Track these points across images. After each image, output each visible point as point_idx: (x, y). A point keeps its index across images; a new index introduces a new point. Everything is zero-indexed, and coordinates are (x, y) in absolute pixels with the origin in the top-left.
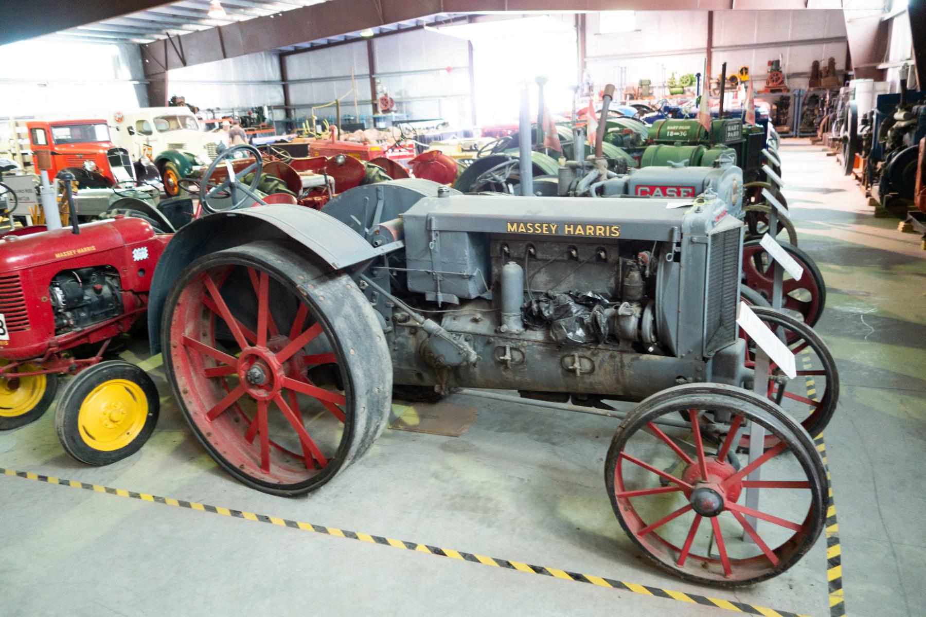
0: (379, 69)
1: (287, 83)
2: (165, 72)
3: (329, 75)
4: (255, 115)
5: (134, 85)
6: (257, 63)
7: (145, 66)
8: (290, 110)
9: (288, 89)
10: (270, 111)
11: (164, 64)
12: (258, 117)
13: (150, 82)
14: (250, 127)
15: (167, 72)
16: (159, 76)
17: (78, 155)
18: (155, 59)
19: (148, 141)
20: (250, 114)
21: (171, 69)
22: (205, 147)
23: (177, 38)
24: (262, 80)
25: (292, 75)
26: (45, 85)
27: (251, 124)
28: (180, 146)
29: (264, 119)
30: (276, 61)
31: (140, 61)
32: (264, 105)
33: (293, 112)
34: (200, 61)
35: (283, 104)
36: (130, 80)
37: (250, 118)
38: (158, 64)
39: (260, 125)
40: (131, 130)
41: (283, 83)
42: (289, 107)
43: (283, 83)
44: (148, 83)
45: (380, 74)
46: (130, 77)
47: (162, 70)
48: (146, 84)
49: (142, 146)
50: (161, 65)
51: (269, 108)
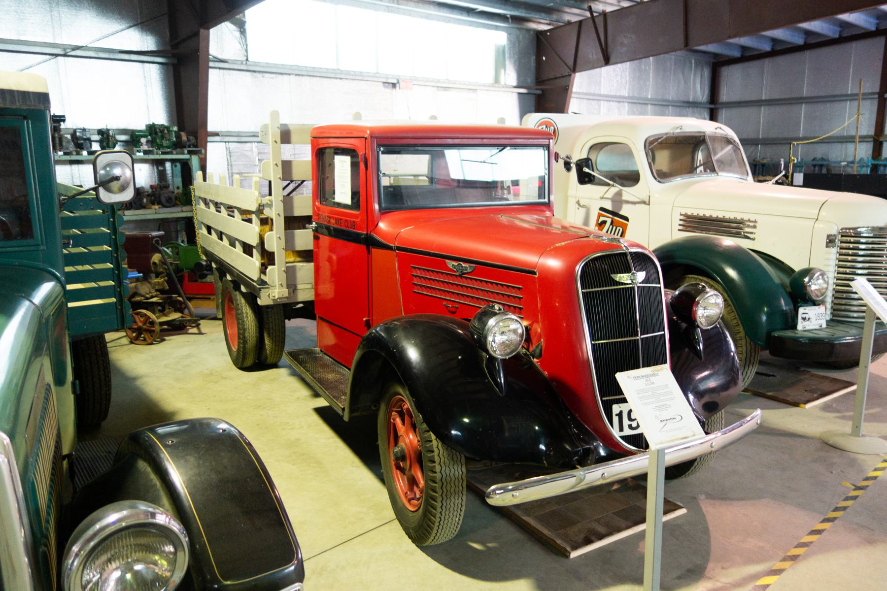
1: (717, 106)
2: (570, 75)
3: (795, 95)
5: (519, 93)
6: (683, 73)
7: (539, 61)
11: (571, 63)
13: (542, 90)
15: (573, 75)
17: (451, 264)
18: (556, 53)
19: (618, 200)
21: (579, 72)
22: (830, 241)
23: (602, 18)
24: (686, 100)
26: (394, 85)
28: (733, 227)
30: (707, 73)
31: (533, 58)
34: (632, 57)
36: (515, 87)
40: (586, 170)
41: (712, 106)
43: (712, 106)
47: (566, 71)
48: (535, 94)
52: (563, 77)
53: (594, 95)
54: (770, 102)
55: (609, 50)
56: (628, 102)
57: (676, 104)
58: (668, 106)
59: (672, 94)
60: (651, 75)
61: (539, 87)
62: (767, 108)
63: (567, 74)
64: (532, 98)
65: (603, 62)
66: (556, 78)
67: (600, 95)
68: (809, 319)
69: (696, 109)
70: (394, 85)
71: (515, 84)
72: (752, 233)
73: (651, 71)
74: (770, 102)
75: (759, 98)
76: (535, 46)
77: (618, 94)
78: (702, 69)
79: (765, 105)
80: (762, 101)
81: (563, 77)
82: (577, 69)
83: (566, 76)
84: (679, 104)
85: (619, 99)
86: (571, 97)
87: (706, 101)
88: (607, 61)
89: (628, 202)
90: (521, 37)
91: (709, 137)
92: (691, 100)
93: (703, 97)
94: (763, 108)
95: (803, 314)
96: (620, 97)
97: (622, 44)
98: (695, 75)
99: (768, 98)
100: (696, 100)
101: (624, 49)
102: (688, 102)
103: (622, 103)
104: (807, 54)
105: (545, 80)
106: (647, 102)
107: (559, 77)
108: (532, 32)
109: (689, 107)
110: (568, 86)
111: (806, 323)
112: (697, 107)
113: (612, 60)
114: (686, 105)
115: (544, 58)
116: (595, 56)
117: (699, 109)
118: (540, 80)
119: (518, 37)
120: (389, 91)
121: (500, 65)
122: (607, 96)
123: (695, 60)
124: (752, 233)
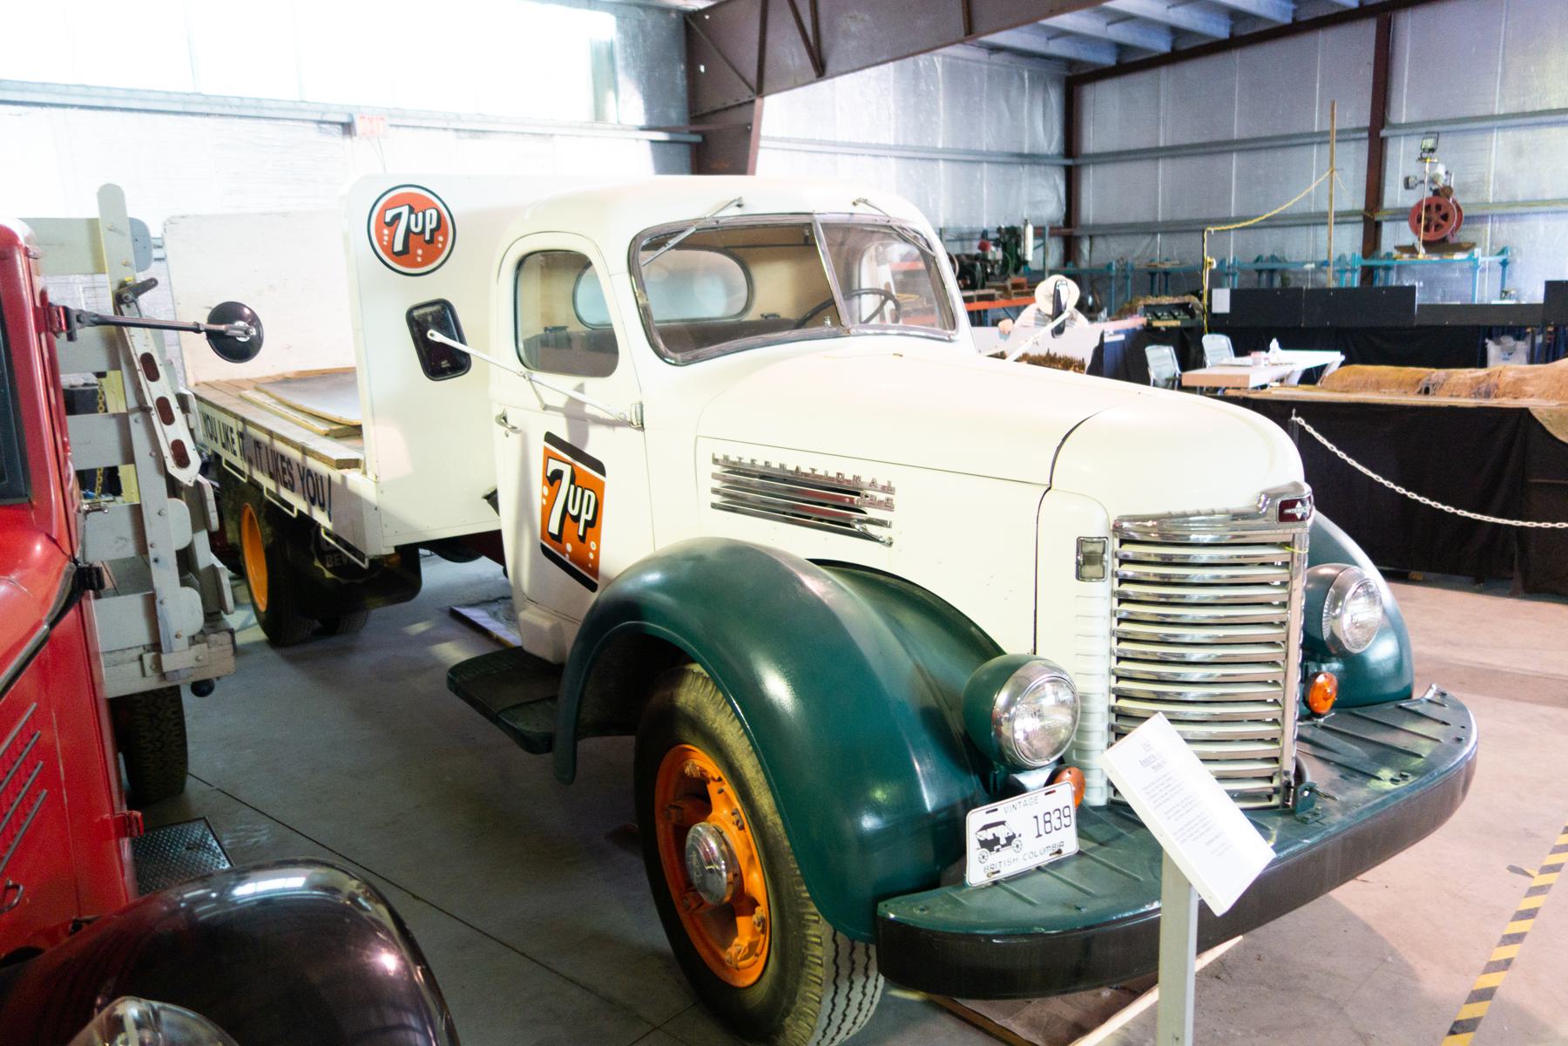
0: (1403, 109)
1: (1079, 161)
2: (752, 102)
3: (1219, 136)
4: (995, 253)
5: (653, 142)
6: (1007, 100)
7: (693, 79)
8: (1078, 238)
9: (1078, 180)
10: (1041, 241)
11: (752, 76)
12: (1005, 257)
14: (983, 287)
15: (758, 101)
16: (736, 117)
19: (576, 415)
20: (983, 247)
22: (1088, 559)
24: (1016, 150)
25: (1093, 139)
27: (987, 277)
29: (1022, 262)
30: (1055, 97)
32: (1026, 223)
33: (1085, 246)
35: (1061, 223)
36: (642, 129)
37: (983, 259)
38: (736, 79)
39: (1009, 283)
40: (437, 336)
41: (1069, 162)
42: (1076, 232)
43: (1069, 162)
44: (697, 138)
45: (1400, 126)
46: (642, 120)
47: (746, 95)
48: (689, 143)
49: (538, 446)
50: (743, 79)
51: (1039, 233)
52: (740, 105)
53: (820, 143)
54: (1173, 152)
55: (825, 44)
56: (896, 157)
57: (994, 159)
58: (980, 162)
59: (987, 139)
60: (941, 103)
61: (695, 128)
62: (1168, 161)
63: (746, 99)
64: (684, 151)
65: (812, 73)
66: (727, 109)
67: (834, 144)
68: (1010, 839)
69: (1036, 168)
70: (348, 128)
71: (642, 122)
72: (882, 523)
73: (941, 94)
74: (1173, 152)
75: (1153, 145)
76: (683, 44)
77: (874, 142)
78: (1046, 90)
79: (1164, 157)
80: (1158, 149)
81: (740, 105)
82: (766, 88)
83: (745, 103)
84: (1000, 159)
85: (877, 151)
86: (758, 147)
87: (1056, 152)
88: (821, 69)
89: (599, 421)
90: (649, 23)
91: (826, 226)
92: (1026, 151)
93: (1049, 146)
94: (1161, 164)
95: (986, 827)
96: (878, 147)
97: (847, 35)
98: (1031, 102)
99: (1169, 144)
100: (1035, 151)
101: (853, 44)
102: (1020, 155)
103: (883, 159)
104: (1237, 57)
105: (707, 114)
106: (934, 156)
107: (733, 107)
108: (673, 15)
109: (1022, 164)
110: (751, 124)
111: (994, 858)
112: (1039, 164)
113: (831, 66)
114: (1019, 160)
115: (702, 69)
116: (797, 61)
117: (1043, 168)
118: (698, 113)
119: (641, 24)
120: (336, 138)
121: (604, 79)
122: (849, 145)
123: (1029, 71)
124: (882, 523)
